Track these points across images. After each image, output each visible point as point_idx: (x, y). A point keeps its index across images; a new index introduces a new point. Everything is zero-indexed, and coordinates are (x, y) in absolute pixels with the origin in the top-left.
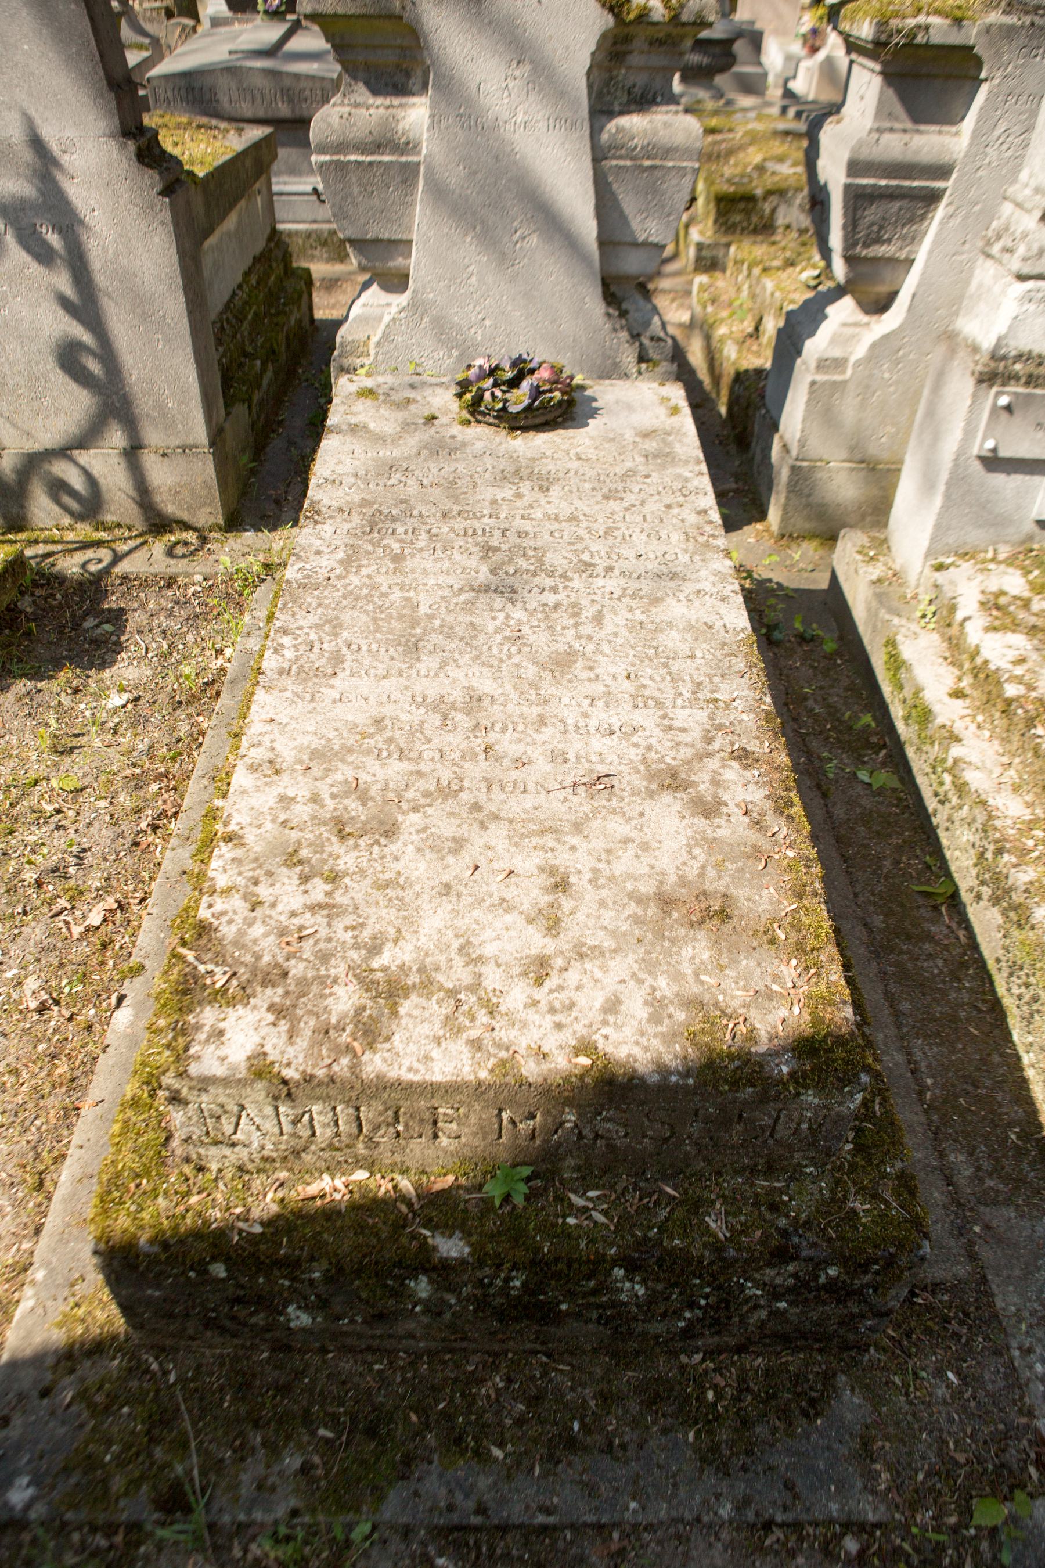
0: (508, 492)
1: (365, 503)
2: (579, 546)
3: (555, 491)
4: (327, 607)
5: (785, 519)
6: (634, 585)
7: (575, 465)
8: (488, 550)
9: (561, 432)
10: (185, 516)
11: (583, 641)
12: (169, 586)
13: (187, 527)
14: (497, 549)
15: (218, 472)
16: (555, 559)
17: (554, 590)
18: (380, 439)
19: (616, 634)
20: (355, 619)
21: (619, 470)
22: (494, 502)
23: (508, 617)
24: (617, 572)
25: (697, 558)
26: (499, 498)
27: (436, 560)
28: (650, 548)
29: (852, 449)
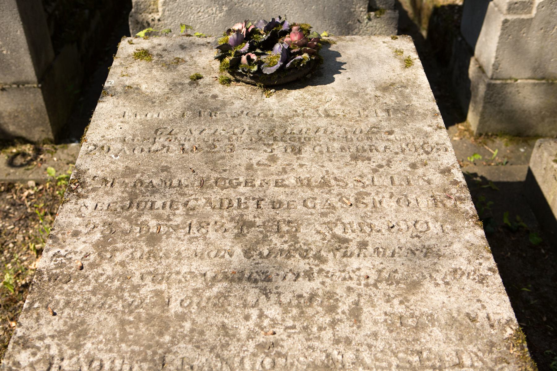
0: (262, 156)
1: (129, 172)
2: (331, 218)
3: (307, 152)
4: (76, 304)
5: (482, 123)
6: (390, 266)
7: (323, 122)
8: (243, 225)
9: (310, 88)
10: (23, 133)
11: (341, 347)
12: (8, 190)
13: (25, 141)
14: (252, 225)
15: (46, 100)
16: (309, 235)
17: (309, 275)
18: (149, 101)
19: (375, 335)
20: (101, 321)
21: (364, 126)
22: (249, 167)
23: (261, 315)
24: (370, 249)
25: (448, 227)
26: (254, 162)
27: (190, 240)
28: (401, 216)
29: (535, 70)
